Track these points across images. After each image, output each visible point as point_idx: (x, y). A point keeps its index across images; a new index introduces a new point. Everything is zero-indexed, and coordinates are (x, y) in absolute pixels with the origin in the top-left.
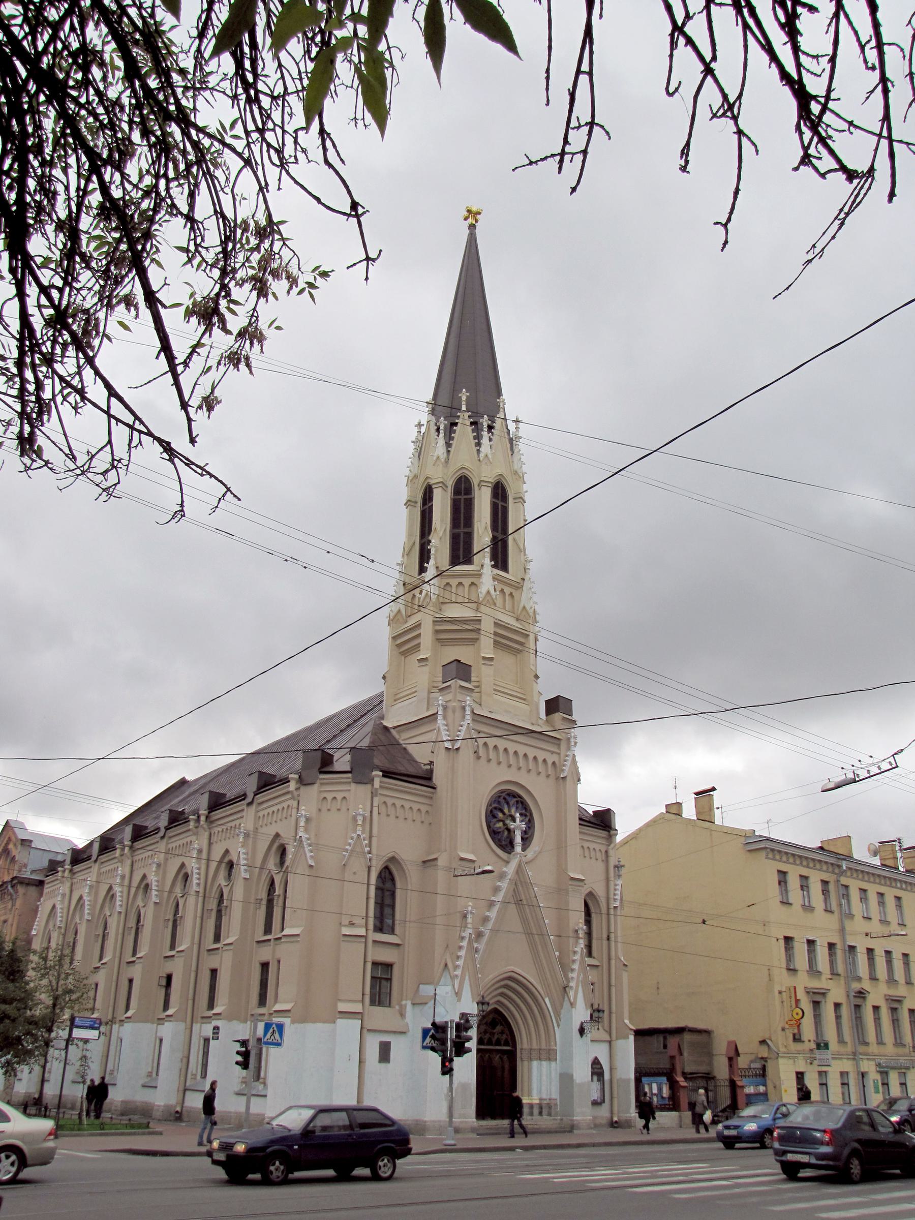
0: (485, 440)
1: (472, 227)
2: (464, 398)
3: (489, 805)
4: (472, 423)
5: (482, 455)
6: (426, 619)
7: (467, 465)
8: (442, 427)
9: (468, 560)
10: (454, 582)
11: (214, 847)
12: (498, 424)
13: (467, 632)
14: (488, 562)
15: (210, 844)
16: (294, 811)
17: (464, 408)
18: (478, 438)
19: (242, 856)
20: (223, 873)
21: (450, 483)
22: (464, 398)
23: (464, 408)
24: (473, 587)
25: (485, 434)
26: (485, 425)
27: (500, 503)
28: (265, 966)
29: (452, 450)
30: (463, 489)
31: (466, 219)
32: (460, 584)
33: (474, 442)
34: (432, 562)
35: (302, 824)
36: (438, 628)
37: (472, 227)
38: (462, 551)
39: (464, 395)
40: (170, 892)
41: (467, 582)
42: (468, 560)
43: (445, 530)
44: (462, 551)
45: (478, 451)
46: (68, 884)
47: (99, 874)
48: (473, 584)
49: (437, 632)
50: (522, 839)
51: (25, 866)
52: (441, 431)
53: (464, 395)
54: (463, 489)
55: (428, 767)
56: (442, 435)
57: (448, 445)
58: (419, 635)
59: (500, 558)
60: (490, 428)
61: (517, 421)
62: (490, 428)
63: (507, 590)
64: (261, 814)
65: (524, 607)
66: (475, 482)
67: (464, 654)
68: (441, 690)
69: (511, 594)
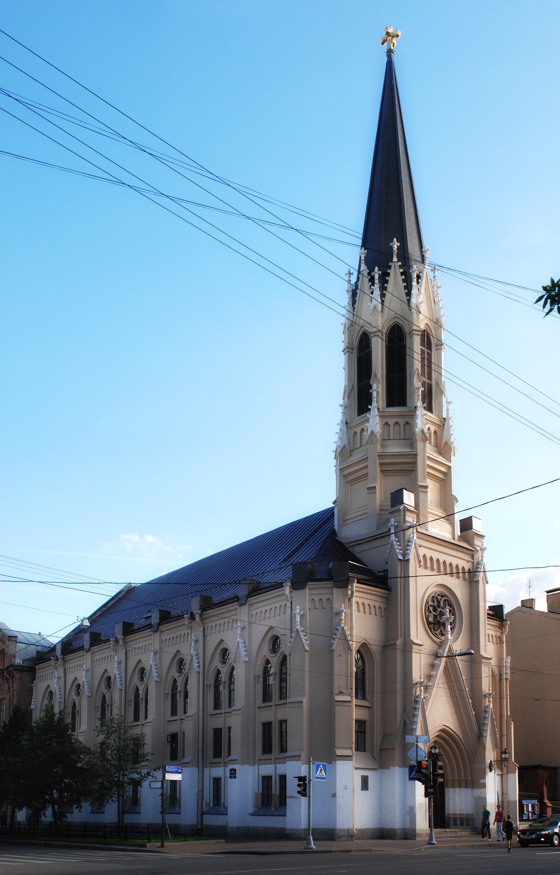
0: (414, 291)
3: (427, 602)
4: (402, 274)
8: (377, 276)
11: (208, 638)
14: (419, 404)
15: (204, 636)
16: (288, 610)
19: (241, 645)
20: (218, 657)
24: (407, 426)
27: (426, 350)
28: (267, 726)
32: (397, 423)
34: (374, 404)
35: (298, 619)
37: (390, 52)
40: (168, 672)
41: (402, 421)
45: (409, 301)
46: (61, 670)
47: (93, 661)
48: (407, 423)
50: (451, 629)
51: (14, 657)
52: (377, 281)
54: (397, 337)
55: (382, 574)
57: (383, 295)
58: (367, 467)
64: (254, 612)
66: (407, 330)
68: (391, 513)
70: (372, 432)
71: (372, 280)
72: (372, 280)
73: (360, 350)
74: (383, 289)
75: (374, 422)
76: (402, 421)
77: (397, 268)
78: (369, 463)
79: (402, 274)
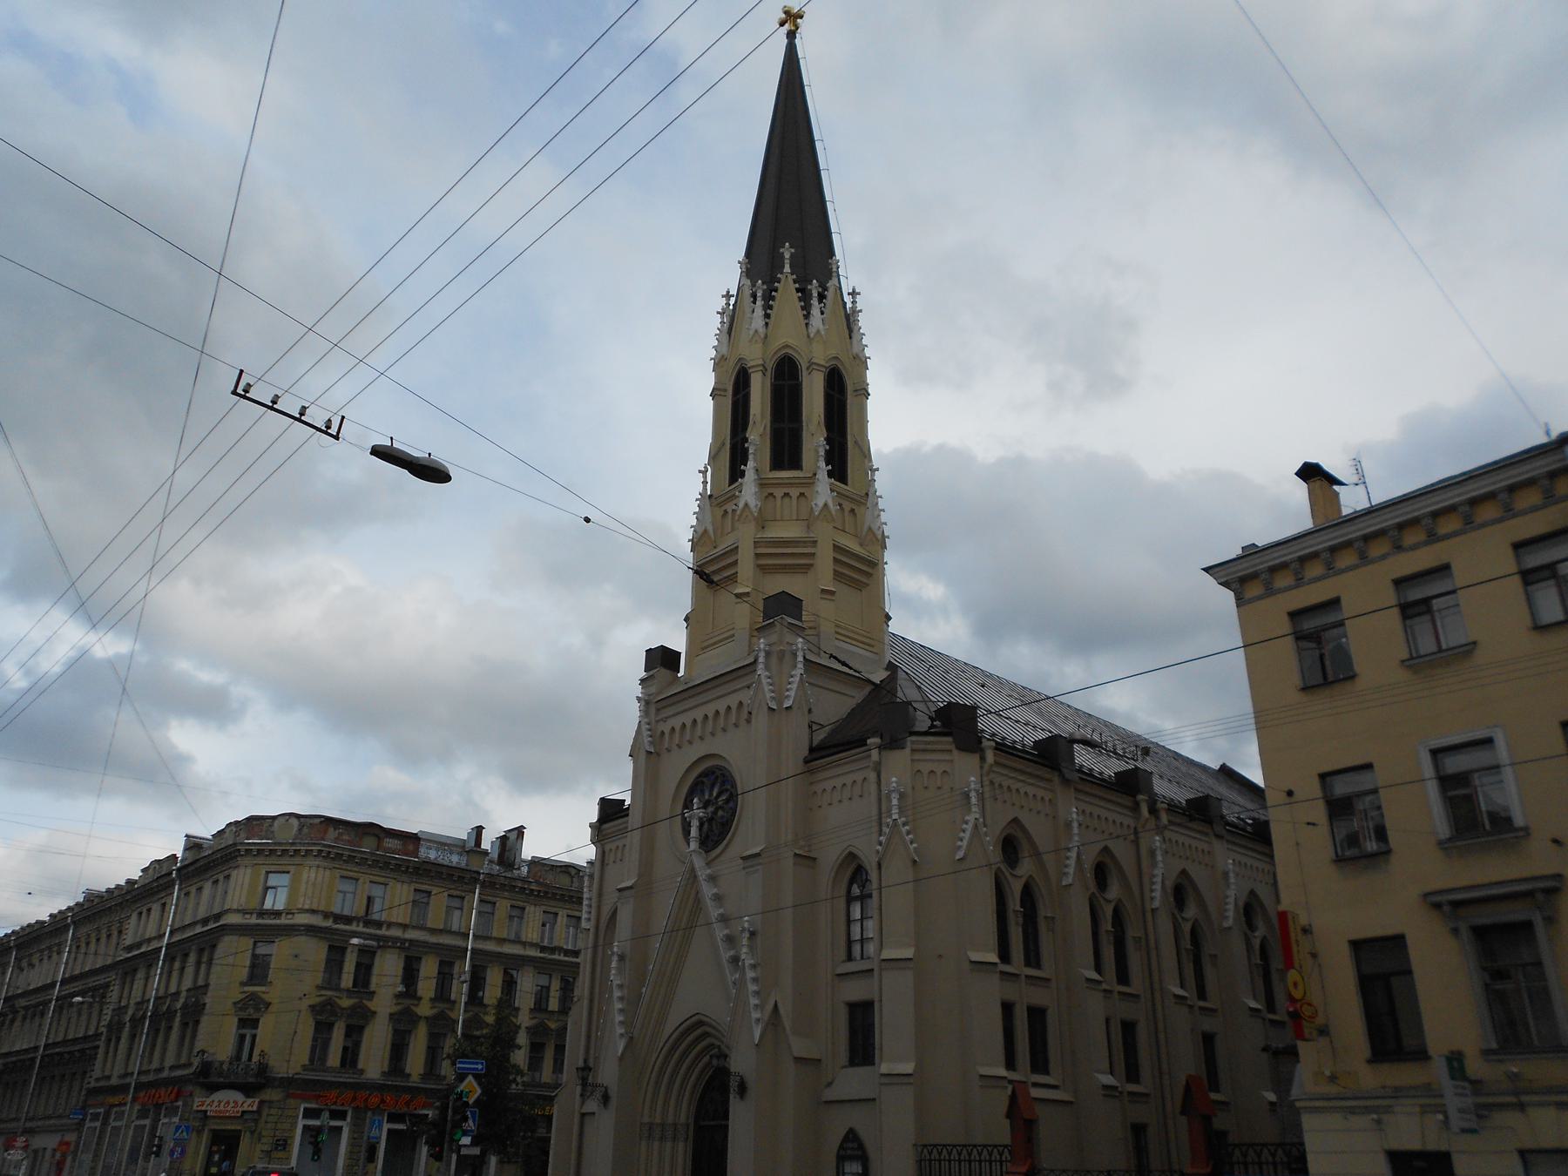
0: (815, 311)
1: (791, 35)
2: (787, 255)
5: (812, 331)
6: (745, 537)
7: (791, 342)
8: (759, 294)
9: (796, 464)
10: (779, 493)
12: (830, 294)
13: (796, 558)
14: (823, 468)
17: (787, 269)
18: (807, 308)
21: (770, 365)
22: (787, 255)
23: (787, 269)
25: (815, 302)
26: (815, 294)
29: (771, 321)
30: (786, 373)
31: (782, 24)
33: (801, 313)
34: (751, 464)
36: (760, 551)
37: (791, 35)
38: (786, 452)
39: (787, 252)
41: (794, 492)
42: (796, 464)
44: (786, 452)
48: (802, 494)
49: (757, 555)
53: (787, 252)
54: (786, 373)
56: (759, 302)
57: (767, 316)
60: (821, 297)
61: (853, 294)
62: (821, 297)
63: (847, 506)
66: (804, 364)
67: (793, 585)
69: (852, 511)
70: (746, 505)
71: (754, 296)
72: (754, 296)
73: (734, 392)
74: (767, 307)
75: (749, 490)
76: (794, 492)
78: (739, 556)
79: (798, 290)
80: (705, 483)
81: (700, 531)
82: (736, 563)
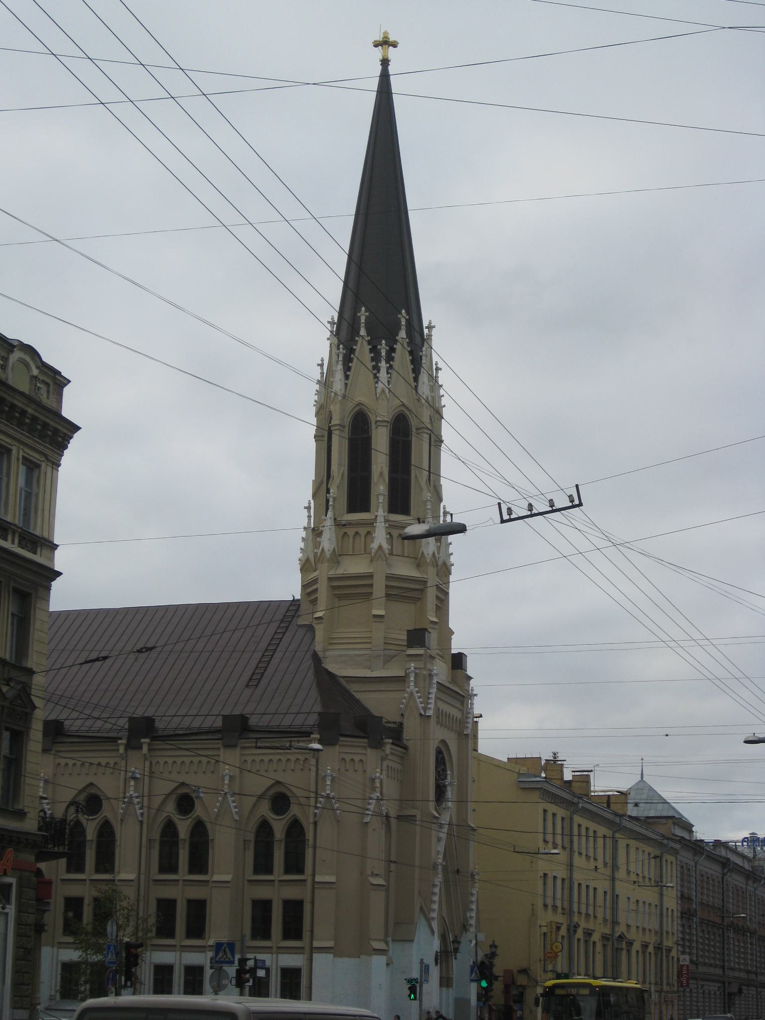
5: (379, 390)
10: (351, 532)
17: (363, 332)
18: (377, 368)
21: (347, 421)
23: (363, 332)
30: (360, 426)
38: (359, 498)
39: (363, 314)
41: (363, 531)
43: (343, 475)
44: (359, 498)
48: (369, 533)
49: (334, 588)
53: (363, 314)
57: (347, 377)
59: (400, 501)
65: (423, 553)
66: (373, 418)
77: (365, 343)
80: (309, 517)
81: (304, 560)
82: (316, 590)
